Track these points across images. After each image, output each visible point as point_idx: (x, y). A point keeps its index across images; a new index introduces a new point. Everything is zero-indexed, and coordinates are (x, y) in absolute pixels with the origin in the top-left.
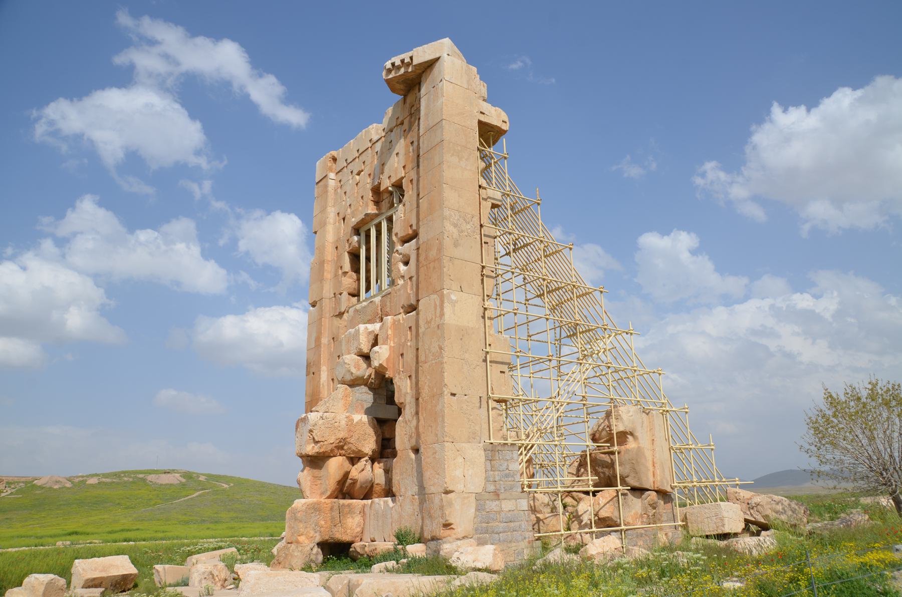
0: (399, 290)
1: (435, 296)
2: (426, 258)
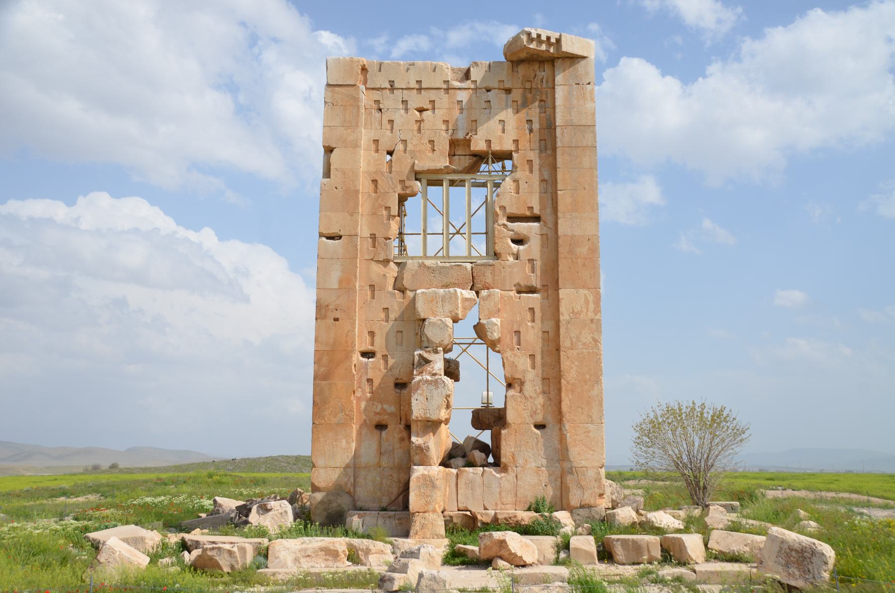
0: (510, 266)
1: (587, 292)
2: (571, 252)
